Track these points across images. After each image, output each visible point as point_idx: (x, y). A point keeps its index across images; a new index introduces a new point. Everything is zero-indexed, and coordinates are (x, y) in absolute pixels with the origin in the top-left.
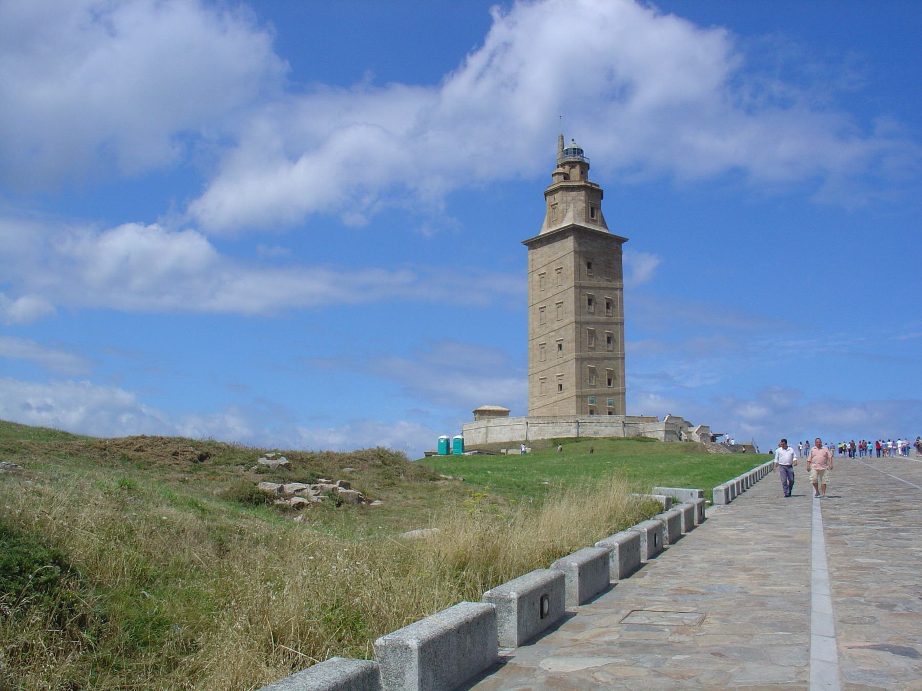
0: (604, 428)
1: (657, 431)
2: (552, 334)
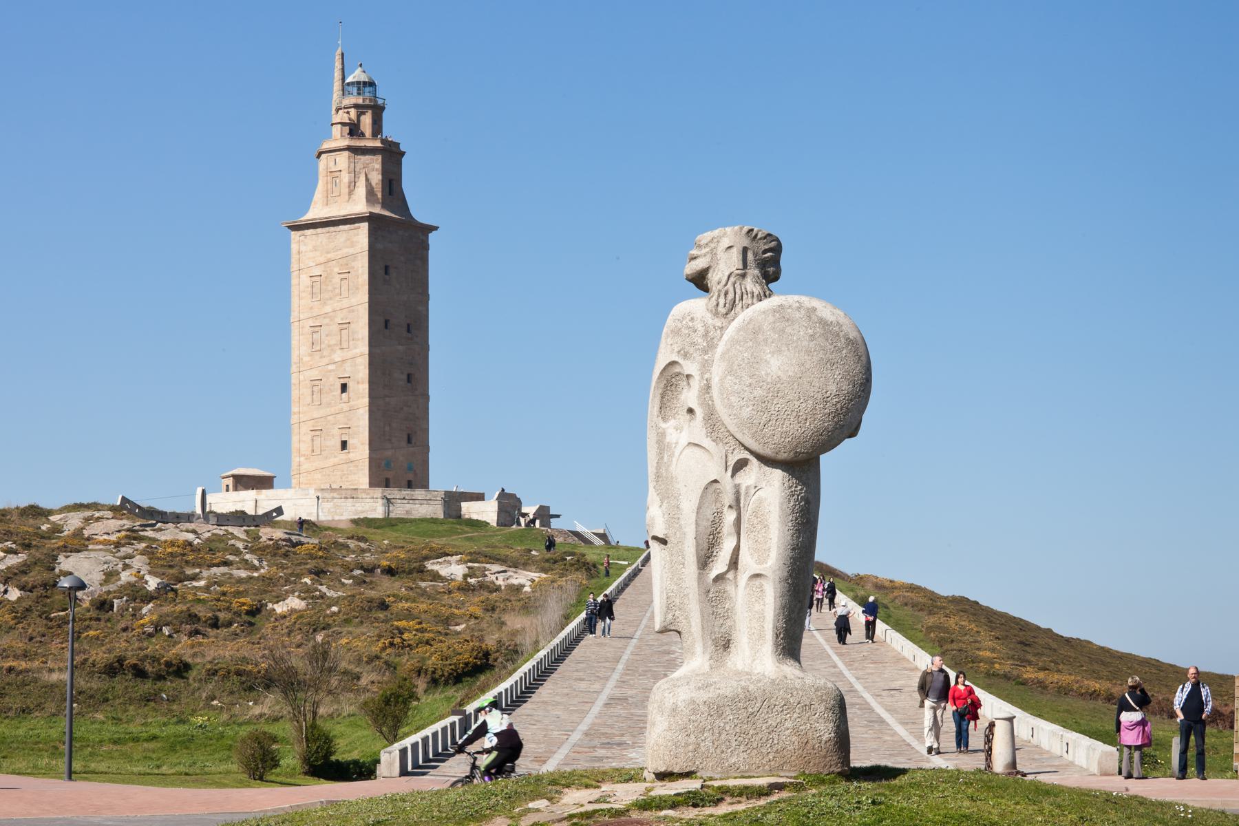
0: (421, 506)
1: (486, 511)
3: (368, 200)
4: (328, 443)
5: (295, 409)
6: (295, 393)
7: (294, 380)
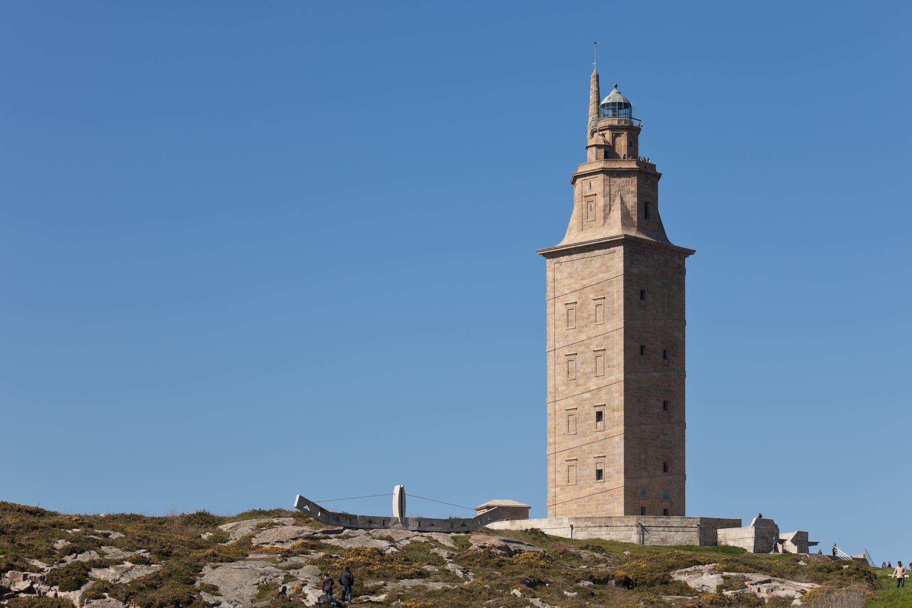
3: (624, 224)
4: (584, 473)
5: (551, 440)
6: (550, 424)
7: (550, 411)
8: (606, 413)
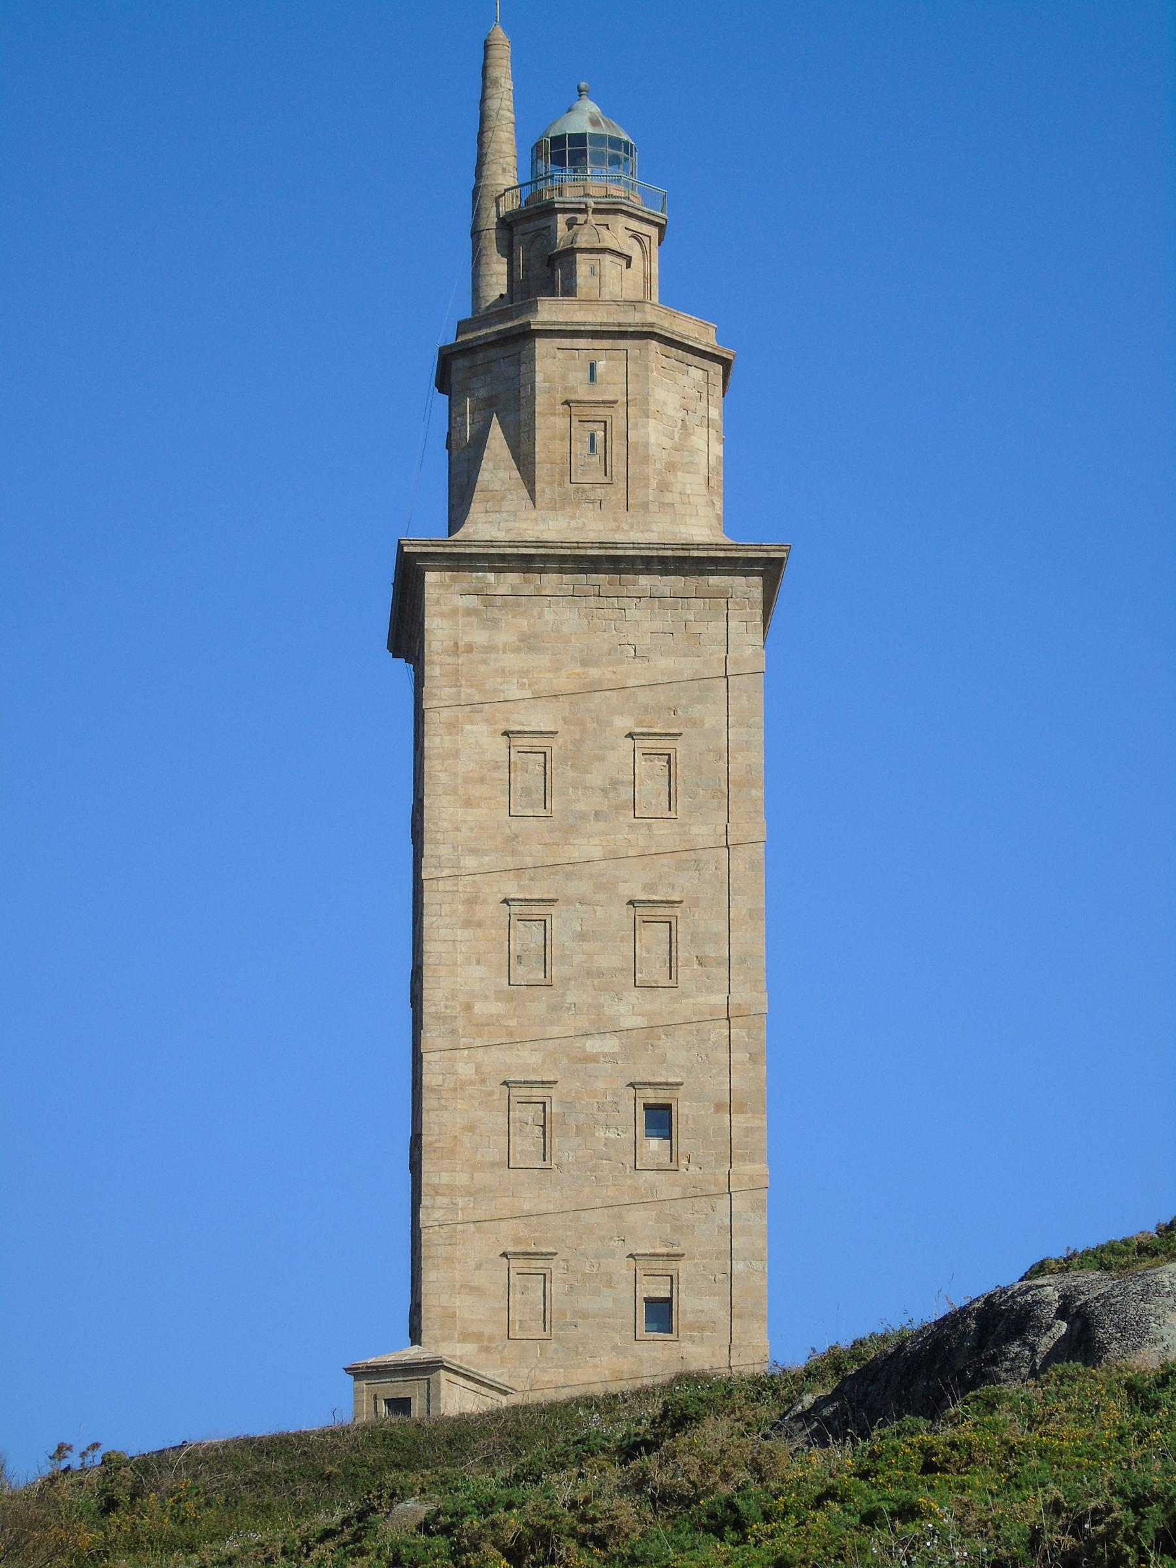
2: (592, 1045)
8: (685, 1111)
